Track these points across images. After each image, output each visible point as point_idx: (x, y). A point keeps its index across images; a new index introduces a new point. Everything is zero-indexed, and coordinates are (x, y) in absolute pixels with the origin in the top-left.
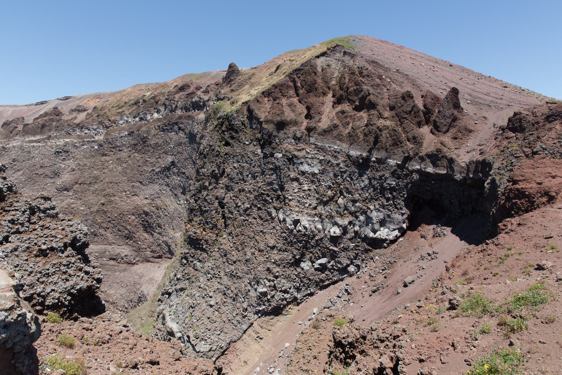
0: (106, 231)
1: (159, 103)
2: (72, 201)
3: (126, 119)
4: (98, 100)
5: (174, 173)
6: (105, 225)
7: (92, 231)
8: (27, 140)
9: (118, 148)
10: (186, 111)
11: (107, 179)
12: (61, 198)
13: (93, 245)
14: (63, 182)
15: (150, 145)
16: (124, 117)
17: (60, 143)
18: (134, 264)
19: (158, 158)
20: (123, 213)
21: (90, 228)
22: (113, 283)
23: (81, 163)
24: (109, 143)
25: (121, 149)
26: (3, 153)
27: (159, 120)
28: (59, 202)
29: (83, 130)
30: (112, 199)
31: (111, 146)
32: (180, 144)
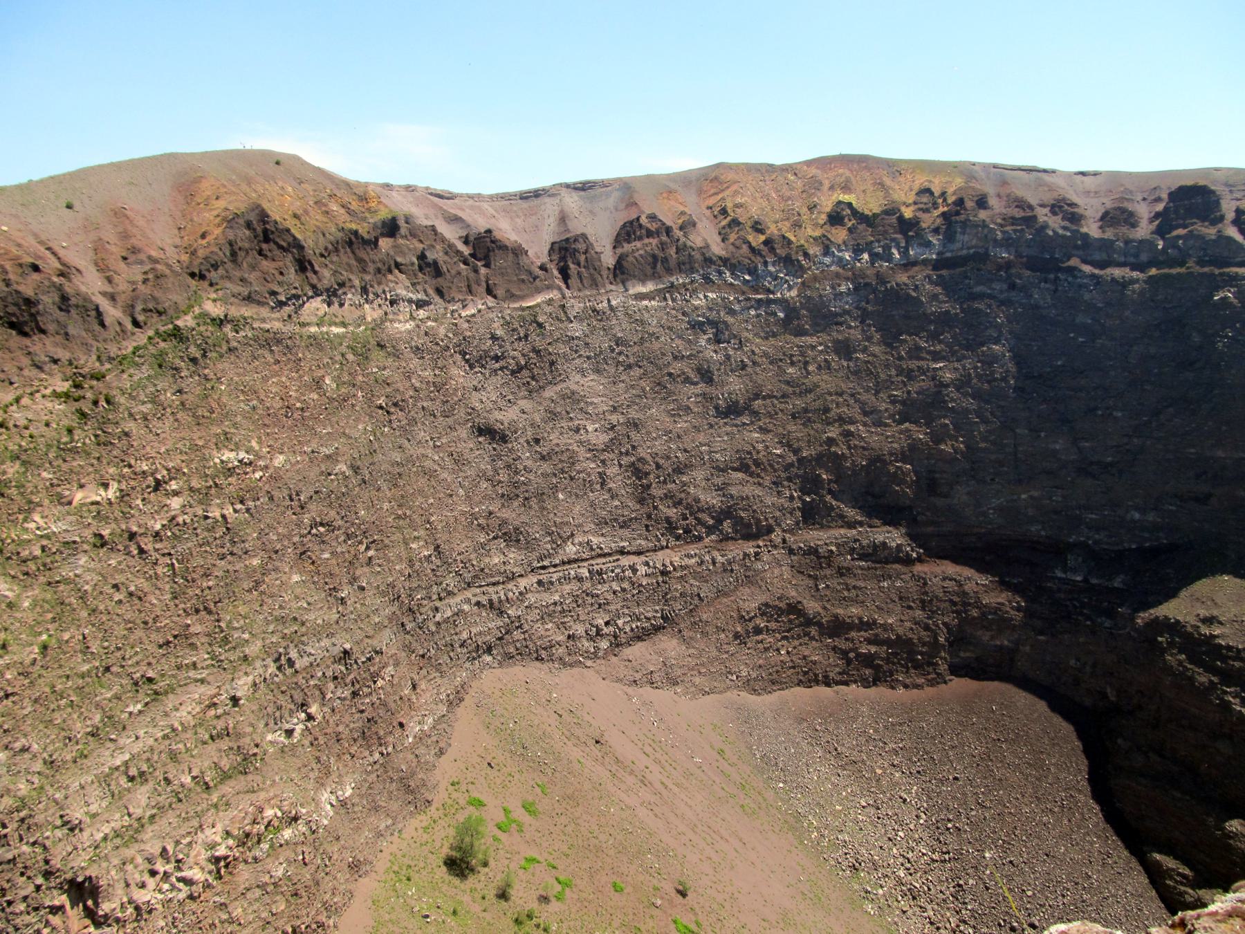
2: (756, 435)
8: (631, 292)
12: (728, 429)
17: (699, 302)
23: (757, 350)
26: (595, 323)
27: (925, 262)
28: (726, 438)
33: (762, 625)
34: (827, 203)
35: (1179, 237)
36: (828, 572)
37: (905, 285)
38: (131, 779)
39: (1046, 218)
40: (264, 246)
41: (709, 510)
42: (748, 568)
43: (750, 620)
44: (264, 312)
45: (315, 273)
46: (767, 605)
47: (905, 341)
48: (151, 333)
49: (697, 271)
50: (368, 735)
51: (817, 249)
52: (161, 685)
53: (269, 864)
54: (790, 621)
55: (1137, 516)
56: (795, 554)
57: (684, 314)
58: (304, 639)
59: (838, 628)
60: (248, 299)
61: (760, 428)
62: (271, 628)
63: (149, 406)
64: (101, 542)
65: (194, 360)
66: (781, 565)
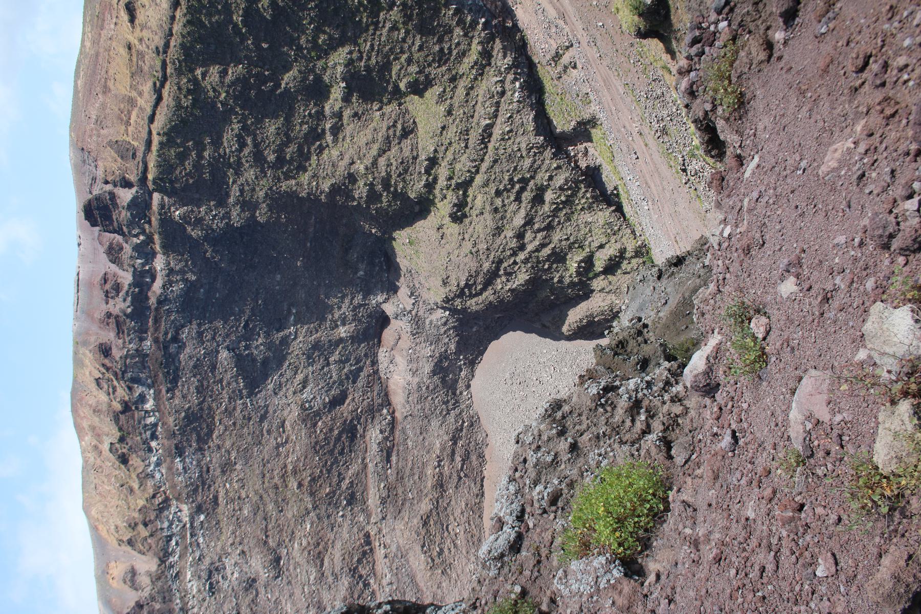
0: (344, 479)
1: (127, 398)
2: (296, 545)
3: (152, 468)
4: (113, 564)
5: (247, 347)
6: (335, 480)
7: (345, 502)
9: (204, 475)
10: (146, 332)
11: (257, 487)
12: (291, 568)
13: (368, 500)
14: (264, 567)
15: (200, 404)
16: (149, 470)
17: (194, 587)
18: (393, 418)
19: (222, 385)
20: (313, 443)
21: (340, 508)
22: (424, 447)
23: (231, 541)
24: (195, 491)
25: (205, 469)
27: (157, 398)
28: (298, 570)
29: (171, 549)
30: (291, 468)
31: (201, 487)
32: (200, 334)
33: (438, 549)
34: (110, 460)
35: (130, 232)
36: (400, 491)
37: (175, 420)
39: (118, 307)
41: (351, 589)
42: (396, 556)
43: (433, 560)
46: (423, 547)
47: (220, 420)
49: (170, 586)
51: (149, 484)
54: (435, 523)
55: (362, 273)
56: (386, 516)
57: (204, 600)
59: (440, 485)
61: (290, 541)
66: (394, 528)
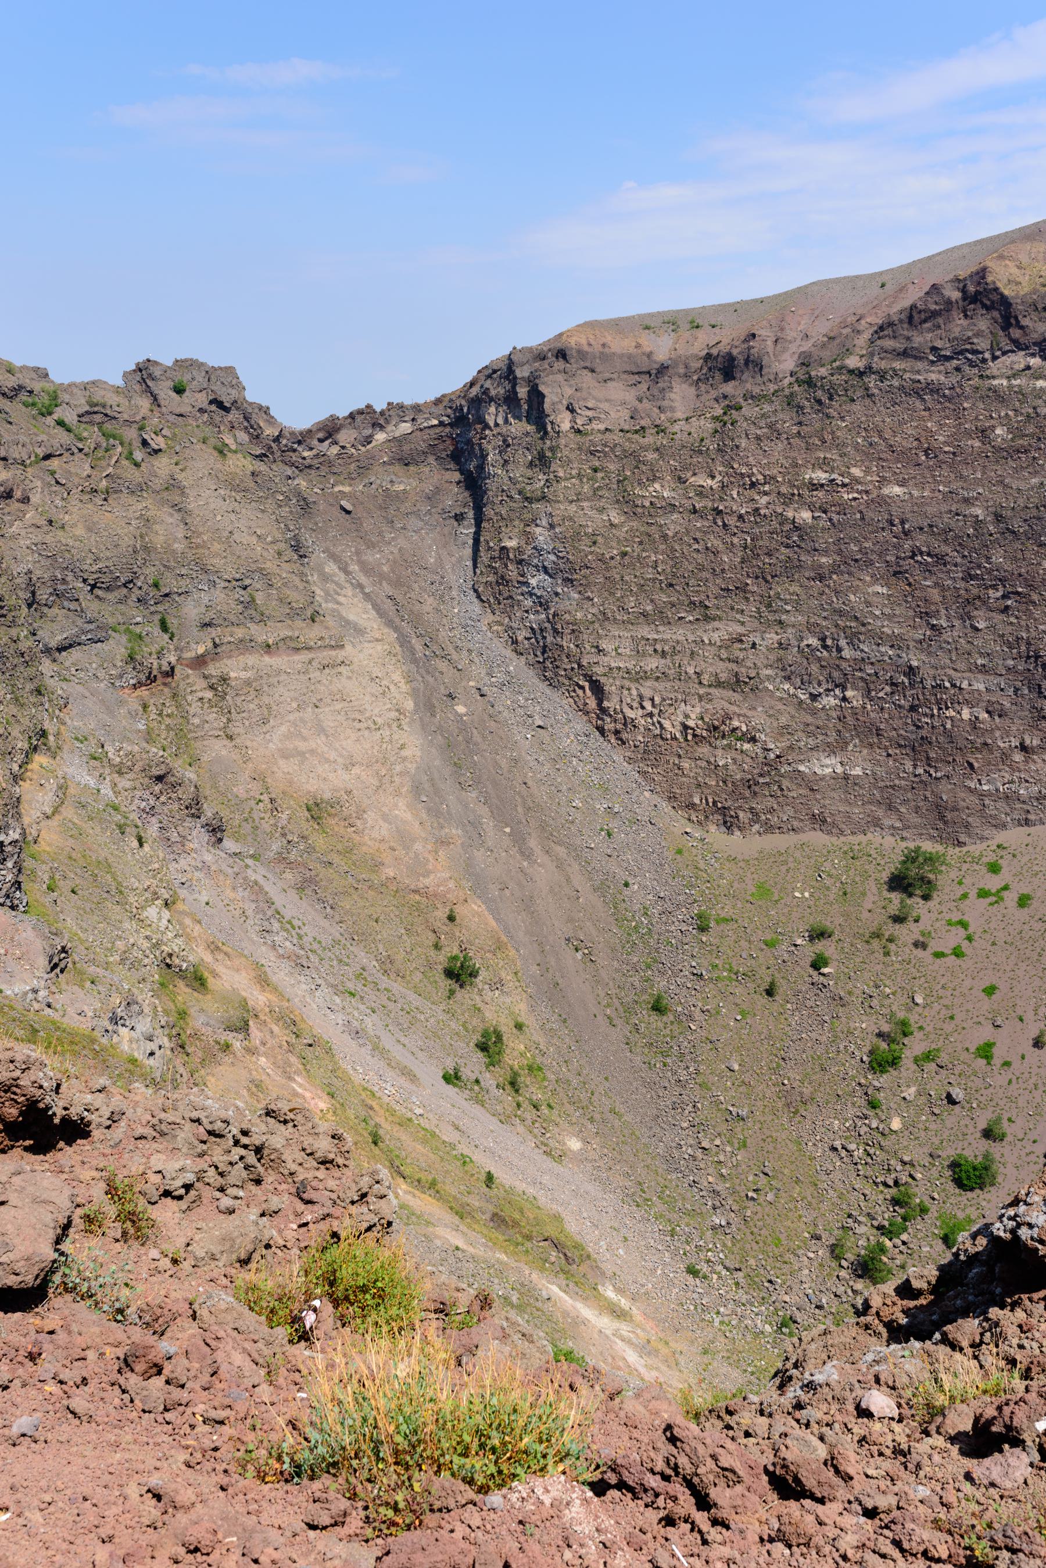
38: (655, 650)
40: (972, 306)
44: (920, 365)
45: (1022, 328)
48: (793, 379)
50: (917, 748)
52: (713, 612)
53: (719, 752)
58: (862, 637)
60: (904, 354)
62: (825, 614)
63: (765, 430)
64: (695, 511)
65: (819, 402)
